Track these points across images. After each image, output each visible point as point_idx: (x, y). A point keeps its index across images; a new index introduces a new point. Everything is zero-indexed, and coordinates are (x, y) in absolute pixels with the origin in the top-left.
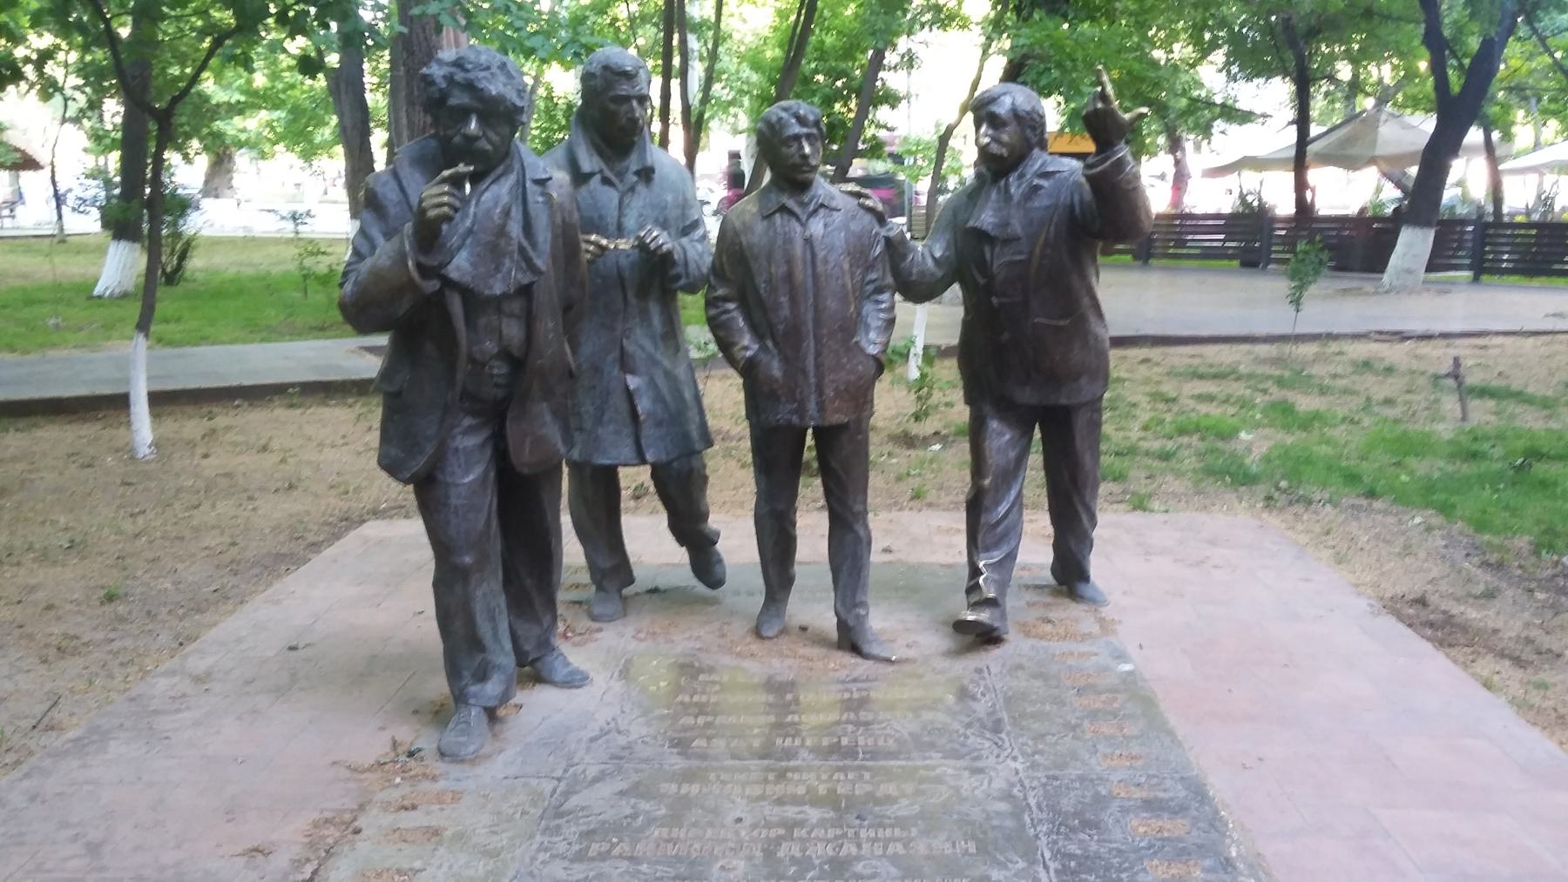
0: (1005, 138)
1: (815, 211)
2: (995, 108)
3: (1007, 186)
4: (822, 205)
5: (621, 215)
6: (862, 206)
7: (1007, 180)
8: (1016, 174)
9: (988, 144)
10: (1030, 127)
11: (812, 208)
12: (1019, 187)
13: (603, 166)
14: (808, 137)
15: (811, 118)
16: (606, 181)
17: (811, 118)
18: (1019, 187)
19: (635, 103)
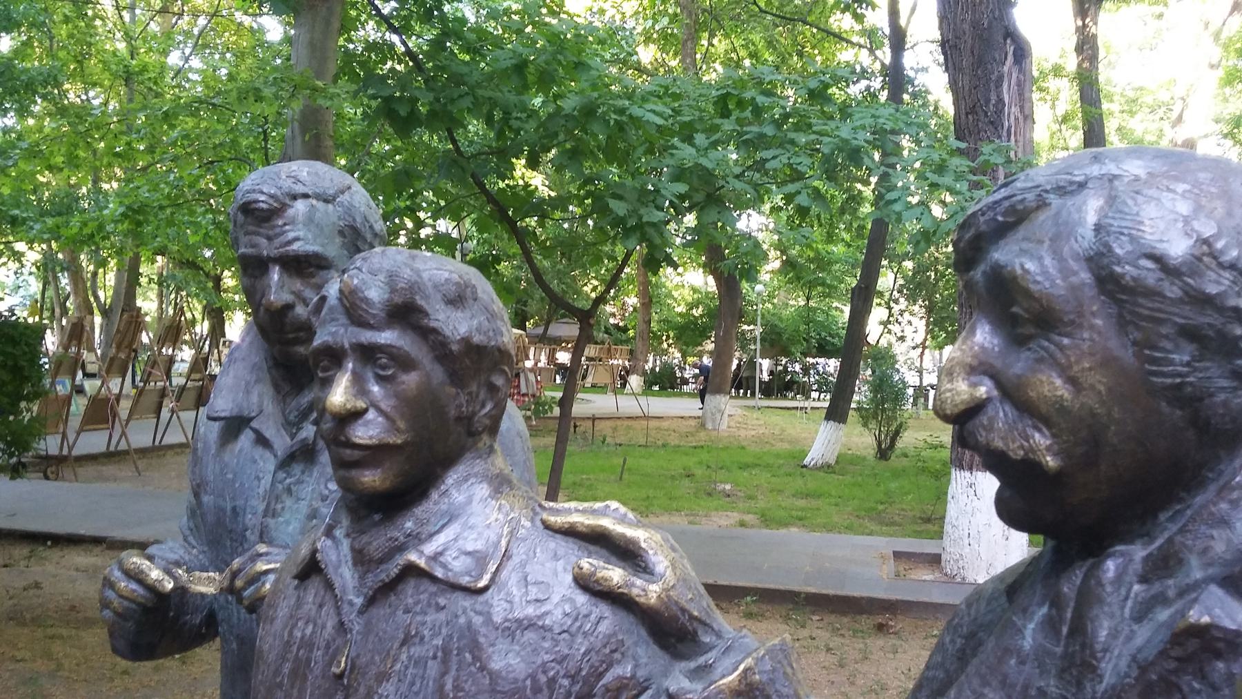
0: (1053, 386)
1: (389, 588)
2: (1005, 254)
3: (1087, 597)
4: (411, 570)
5: (270, 512)
6: (584, 583)
7: (1097, 566)
8: (1139, 552)
9: (975, 409)
10: (1190, 334)
11: (393, 569)
12: (1141, 615)
13: (270, 406)
14: (368, 353)
15: (375, 293)
16: (262, 441)
17: (375, 293)
18: (1141, 615)
19: (275, 274)
